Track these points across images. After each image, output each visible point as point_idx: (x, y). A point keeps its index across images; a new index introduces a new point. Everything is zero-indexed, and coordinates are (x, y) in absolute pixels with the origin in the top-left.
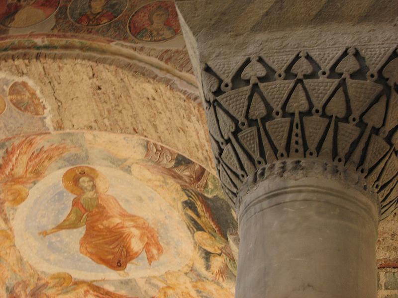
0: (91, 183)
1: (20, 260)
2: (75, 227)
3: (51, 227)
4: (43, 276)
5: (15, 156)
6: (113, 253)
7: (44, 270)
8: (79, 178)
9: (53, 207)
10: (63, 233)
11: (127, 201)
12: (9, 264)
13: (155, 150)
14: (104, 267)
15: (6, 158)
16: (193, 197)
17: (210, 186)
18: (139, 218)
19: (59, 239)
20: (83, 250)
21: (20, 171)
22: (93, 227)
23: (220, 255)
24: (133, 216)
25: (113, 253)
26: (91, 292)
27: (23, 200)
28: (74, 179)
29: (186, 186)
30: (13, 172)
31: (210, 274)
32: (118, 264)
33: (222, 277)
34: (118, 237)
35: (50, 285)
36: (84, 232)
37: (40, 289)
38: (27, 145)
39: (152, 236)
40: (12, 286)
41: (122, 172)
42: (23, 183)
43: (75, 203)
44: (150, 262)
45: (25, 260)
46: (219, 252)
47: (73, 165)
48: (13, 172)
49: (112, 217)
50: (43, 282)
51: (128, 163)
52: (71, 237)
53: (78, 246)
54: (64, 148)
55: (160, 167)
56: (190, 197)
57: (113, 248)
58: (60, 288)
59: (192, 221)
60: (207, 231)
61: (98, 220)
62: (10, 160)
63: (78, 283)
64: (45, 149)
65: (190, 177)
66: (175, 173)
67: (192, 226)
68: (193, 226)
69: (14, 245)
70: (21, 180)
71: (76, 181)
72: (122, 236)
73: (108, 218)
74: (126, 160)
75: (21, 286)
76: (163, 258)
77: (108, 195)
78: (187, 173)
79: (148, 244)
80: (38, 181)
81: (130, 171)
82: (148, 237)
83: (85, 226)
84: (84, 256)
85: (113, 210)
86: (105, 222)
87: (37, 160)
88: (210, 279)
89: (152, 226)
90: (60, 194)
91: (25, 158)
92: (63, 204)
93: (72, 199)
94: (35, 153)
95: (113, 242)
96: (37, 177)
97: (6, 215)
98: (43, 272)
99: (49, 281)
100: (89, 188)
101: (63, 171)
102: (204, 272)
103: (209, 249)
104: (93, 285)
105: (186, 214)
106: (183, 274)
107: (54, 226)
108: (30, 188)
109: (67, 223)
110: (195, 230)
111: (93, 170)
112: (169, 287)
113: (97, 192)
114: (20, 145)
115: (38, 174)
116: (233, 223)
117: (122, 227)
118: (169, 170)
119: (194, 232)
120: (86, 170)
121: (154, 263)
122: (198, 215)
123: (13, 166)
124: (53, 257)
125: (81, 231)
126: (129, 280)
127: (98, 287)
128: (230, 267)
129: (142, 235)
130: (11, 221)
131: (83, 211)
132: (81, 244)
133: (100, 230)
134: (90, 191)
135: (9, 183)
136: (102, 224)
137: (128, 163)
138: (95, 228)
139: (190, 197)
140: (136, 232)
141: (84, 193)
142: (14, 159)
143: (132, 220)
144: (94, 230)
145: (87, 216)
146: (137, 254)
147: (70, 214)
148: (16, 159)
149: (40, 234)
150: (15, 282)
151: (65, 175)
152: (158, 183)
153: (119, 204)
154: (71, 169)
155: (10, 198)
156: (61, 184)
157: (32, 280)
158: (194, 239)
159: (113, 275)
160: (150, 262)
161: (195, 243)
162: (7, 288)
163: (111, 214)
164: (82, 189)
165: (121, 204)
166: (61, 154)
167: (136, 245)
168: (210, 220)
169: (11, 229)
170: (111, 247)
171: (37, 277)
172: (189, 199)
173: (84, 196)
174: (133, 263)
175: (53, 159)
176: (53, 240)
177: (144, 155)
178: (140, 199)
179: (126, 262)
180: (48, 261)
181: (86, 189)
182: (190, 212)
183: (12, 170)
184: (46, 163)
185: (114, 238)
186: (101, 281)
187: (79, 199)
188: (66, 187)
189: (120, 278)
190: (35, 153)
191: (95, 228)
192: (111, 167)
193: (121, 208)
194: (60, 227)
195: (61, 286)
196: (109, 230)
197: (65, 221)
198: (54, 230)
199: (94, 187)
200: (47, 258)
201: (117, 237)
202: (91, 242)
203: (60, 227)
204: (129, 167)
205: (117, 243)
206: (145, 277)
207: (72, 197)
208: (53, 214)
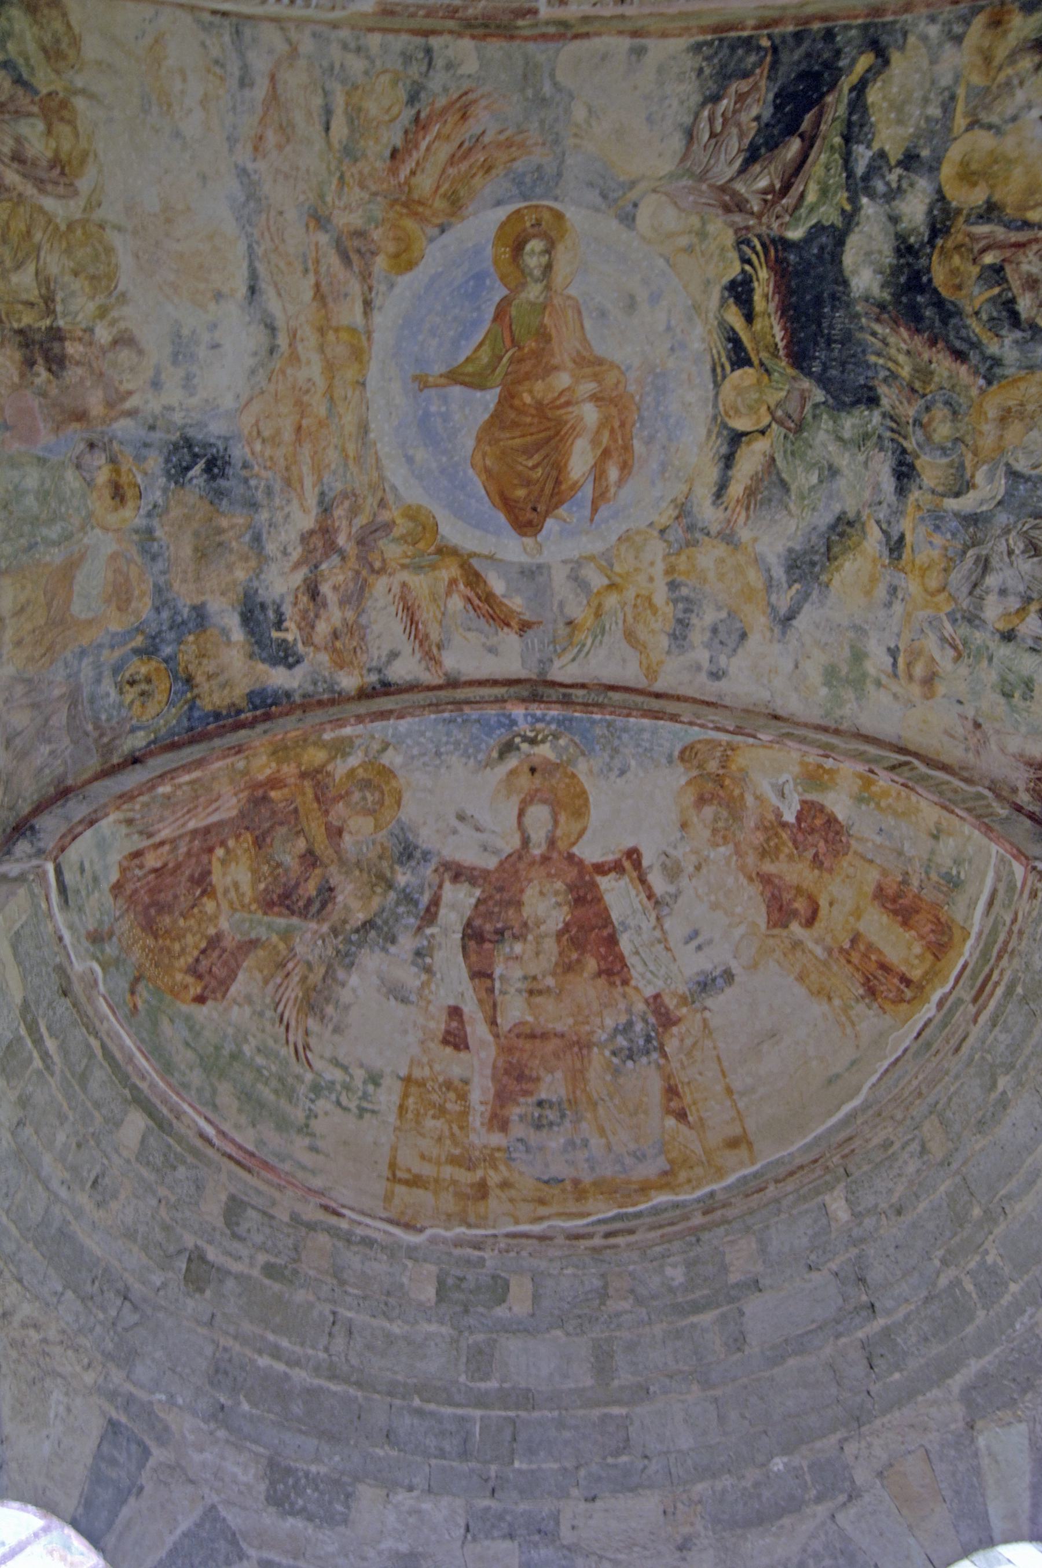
0: (544, 260)
1: (364, 428)
2: (482, 387)
3: (439, 368)
4: (390, 498)
5: (428, 139)
6: (528, 483)
7: (398, 482)
8: (525, 242)
9: (457, 311)
10: (457, 391)
11: (603, 314)
12: (342, 427)
13: (707, 136)
14: (501, 518)
15: (411, 136)
16: (754, 258)
17: (811, 197)
18: (613, 365)
19: (443, 409)
20: (479, 456)
21: (425, 183)
22: (512, 397)
23: (763, 433)
24: (600, 362)
25: (528, 483)
26: (462, 586)
27: (410, 265)
28: (514, 241)
29: (747, 228)
30: (414, 181)
31: (720, 514)
32: (526, 521)
33: (748, 509)
34: (552, 432)
35: (397, 532)
36: (492, 406)
37: (378, 534)
38: (457, 117)
39: (623, 425)
40: (332, 495)
41: (614, 224)
42: (423, 220)
43: (501, 313)
44: (595, 510)
45: (372, 435)
46: (766, 420)
47: (525, 197)
48: (414, 181)
49: (556, 368)
50: (385, 516)
51: (633, 195)
52: (467, 410)
53: (471, 443)
54: (522, 145)
55: (704, 187)
56: (749, 262)
57: (535, 467)
58: (410, 550)
59: (729, 340)
60: (756, 362)
61: (527, 376)
62: (416, 146)
63: (446, 551)
64: (486, 139)
65: (765, 192)
66: (734, 194)
67: (724, 359)
68: (729, 358)
69: (364, 384)
70: (420, 209)
71: (518, 248)
72: (558, 433)
73: (551, 369)
74: (633, 184)
75: (347, 504)
76: (626, 494)
77: (569, 297)
78: (763, 183)
79: (606, 453)
80: (450, 225)
81: (634, 219)
82: (612, 431)
83: (498, 390)
84: (476, 478)
85: (564, 348)
86: (539, 386)
87: (464, 166)
88: (714, 529)
89: (632, 388)
90: (479, 278)
91: (444, 151)
92: (478, 309)
93: (497, 299)
94: (466, 145)
95: (538, 447)
96: (453, 214)
97: (370, 289)
98: (394, 488)
99: (398, 521)
100: (537, 273)
101: (502, 213)
102: (708, 514)
103: (741, 424)
104: (470, 566)
105: (722, 323)
106: (655, 533)
107: (444, 370)
108: (431, 240)
109: (470, 369)
110: (728, 367)
111: (559, 216)
112: (612, 586)
113: (548, 288)
114: (444, 111)
115: (455, 204)
116: (834, 297)
117: (568, 404)
118: (723, 189)
119: (724, 377)
120: (546, 215)
121: (604, 511)
122: (749, 318)
123: (418, 164)
124: (421, 455)
125: (491, 397)
126: (539, 567)
127: (477, 575)
128: (780, 463)
129: (601, 426)
130: (376, 312)
131: (508, 343)
132: (479, 440)
133: (521, 411)
134: (537, 281)
135: (398, 208)
136: (530, 392)
137: (633, 195)
138: (516, 402)
139: (749, 262)
140: (590, 414)
141: (524, 285)
142: (423, 145)
143: (596, 377)
144: (511, 406)
145: (511, 361)
146: (575, 487)
147: (481, 345)
148: (428, 149)
149: (416, 378)
150: (339, 486)
151: (503, 225)
152: (683, 241)
153: (582, 327)
154: (518, 211)
155: (391, 247)
156: (489, 251)
157: (370, 500)
158: (715, 405)
159: (513, 548)
160: (595, 510)
161: (715, 418)
162: (322, 494)
163: (555, 361)
164: (523, 272)
165: (587, 325)
166: (514, 160)
167: (579, 461)
168: (774, 320)
169: (369, 334)
170: (530, 464)
171: (380, 494)
172: (743, 271)
173: (523, 295)
174: (556, 517)
175: (494, 172)
176: (433, 409)
177: (679, 156)
178: (631, 305)
179: (547, 514)
180: (410, 460)
181: (531, 274)
182: (734, 318)
183: (413, 173)
184: (477, 181)
185: (542, 435)
186: (487, 557)
187: (510, 304)
188: (496, 262)
189: (524, 559)
190: (466, 145)
191: (516, 402)
192: (597, 210)
193: (584, 340)
194: (454, 377)
195: (414, 544)
196: (540, 406)
197: (468, 360)
198: (443, 381)
199: (548, 268)
200: (411, 452)
201: (550, 433)
202: (498, 441)
203: (454, 377)
204: (635, 205)
205: (543, 452)
206: (571, 561)
207: (500, 292)
208: (451, 333)
